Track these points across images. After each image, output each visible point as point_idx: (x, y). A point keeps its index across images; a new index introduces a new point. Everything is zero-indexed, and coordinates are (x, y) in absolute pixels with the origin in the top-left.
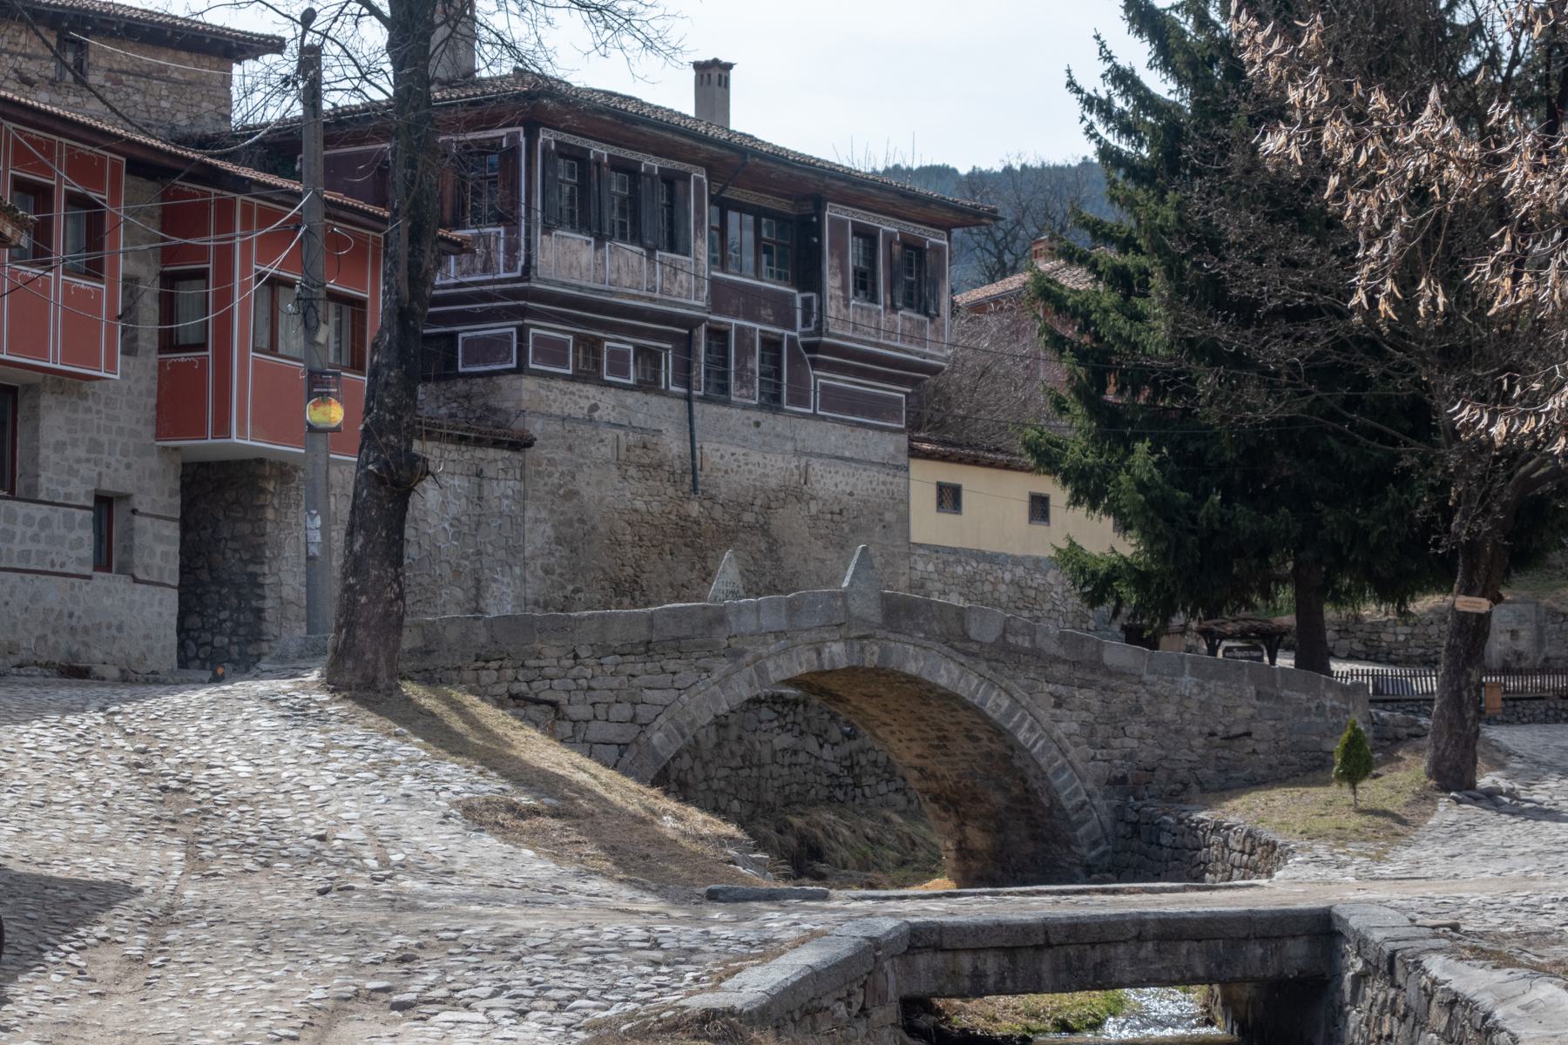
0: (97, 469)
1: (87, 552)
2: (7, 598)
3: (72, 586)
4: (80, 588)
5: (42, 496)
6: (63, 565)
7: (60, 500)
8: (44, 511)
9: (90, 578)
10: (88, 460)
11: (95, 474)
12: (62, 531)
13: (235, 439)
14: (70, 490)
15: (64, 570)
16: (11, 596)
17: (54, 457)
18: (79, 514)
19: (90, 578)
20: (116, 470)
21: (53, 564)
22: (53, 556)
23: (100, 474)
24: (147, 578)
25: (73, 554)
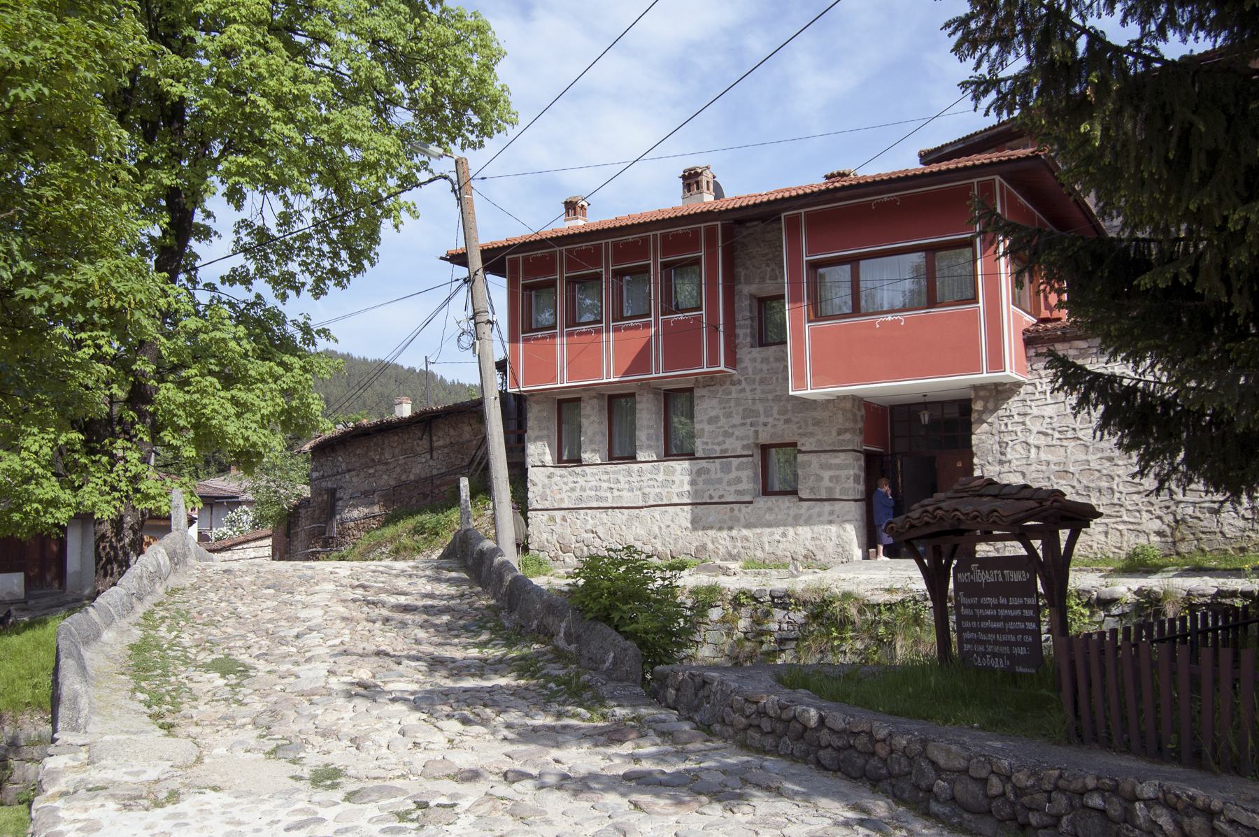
0: (753, 429)
1: (746, 485)
2: (670, 523)
3: (732, 510)
4: (740, 510)
5: (697, 455)
6: (722, 496)
7: (718, 455)
8: (703, 463)
9: (751, 503)
10: (744, 424)
11: (751, 433)
12: (720, 475)
13: (1008, 372)
14: (724, 447)
15: (723, 500)
16: (672, 521)
17: (707, 428)
18: (735, 462)
19: (751, 503)
20: (774, 426)
21: (711, 497)
22: (711, 492)
23: (756, 432)
24: (814, 497)
25: (733, 488)
